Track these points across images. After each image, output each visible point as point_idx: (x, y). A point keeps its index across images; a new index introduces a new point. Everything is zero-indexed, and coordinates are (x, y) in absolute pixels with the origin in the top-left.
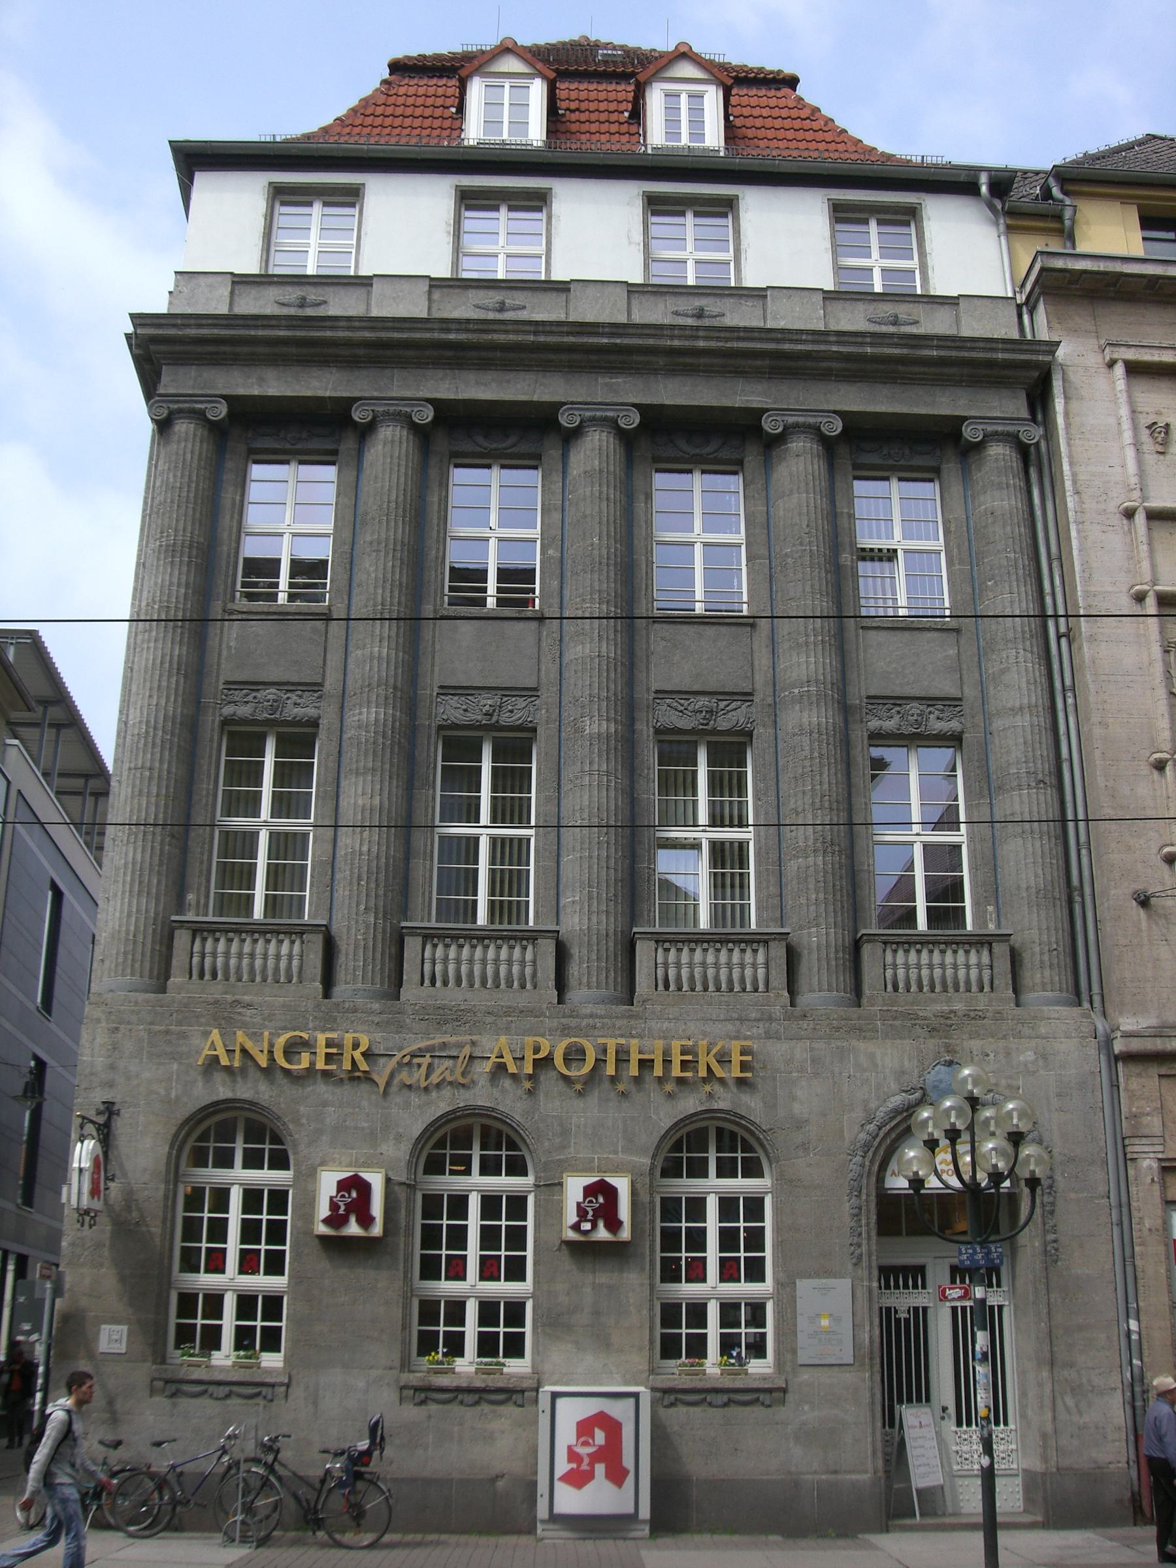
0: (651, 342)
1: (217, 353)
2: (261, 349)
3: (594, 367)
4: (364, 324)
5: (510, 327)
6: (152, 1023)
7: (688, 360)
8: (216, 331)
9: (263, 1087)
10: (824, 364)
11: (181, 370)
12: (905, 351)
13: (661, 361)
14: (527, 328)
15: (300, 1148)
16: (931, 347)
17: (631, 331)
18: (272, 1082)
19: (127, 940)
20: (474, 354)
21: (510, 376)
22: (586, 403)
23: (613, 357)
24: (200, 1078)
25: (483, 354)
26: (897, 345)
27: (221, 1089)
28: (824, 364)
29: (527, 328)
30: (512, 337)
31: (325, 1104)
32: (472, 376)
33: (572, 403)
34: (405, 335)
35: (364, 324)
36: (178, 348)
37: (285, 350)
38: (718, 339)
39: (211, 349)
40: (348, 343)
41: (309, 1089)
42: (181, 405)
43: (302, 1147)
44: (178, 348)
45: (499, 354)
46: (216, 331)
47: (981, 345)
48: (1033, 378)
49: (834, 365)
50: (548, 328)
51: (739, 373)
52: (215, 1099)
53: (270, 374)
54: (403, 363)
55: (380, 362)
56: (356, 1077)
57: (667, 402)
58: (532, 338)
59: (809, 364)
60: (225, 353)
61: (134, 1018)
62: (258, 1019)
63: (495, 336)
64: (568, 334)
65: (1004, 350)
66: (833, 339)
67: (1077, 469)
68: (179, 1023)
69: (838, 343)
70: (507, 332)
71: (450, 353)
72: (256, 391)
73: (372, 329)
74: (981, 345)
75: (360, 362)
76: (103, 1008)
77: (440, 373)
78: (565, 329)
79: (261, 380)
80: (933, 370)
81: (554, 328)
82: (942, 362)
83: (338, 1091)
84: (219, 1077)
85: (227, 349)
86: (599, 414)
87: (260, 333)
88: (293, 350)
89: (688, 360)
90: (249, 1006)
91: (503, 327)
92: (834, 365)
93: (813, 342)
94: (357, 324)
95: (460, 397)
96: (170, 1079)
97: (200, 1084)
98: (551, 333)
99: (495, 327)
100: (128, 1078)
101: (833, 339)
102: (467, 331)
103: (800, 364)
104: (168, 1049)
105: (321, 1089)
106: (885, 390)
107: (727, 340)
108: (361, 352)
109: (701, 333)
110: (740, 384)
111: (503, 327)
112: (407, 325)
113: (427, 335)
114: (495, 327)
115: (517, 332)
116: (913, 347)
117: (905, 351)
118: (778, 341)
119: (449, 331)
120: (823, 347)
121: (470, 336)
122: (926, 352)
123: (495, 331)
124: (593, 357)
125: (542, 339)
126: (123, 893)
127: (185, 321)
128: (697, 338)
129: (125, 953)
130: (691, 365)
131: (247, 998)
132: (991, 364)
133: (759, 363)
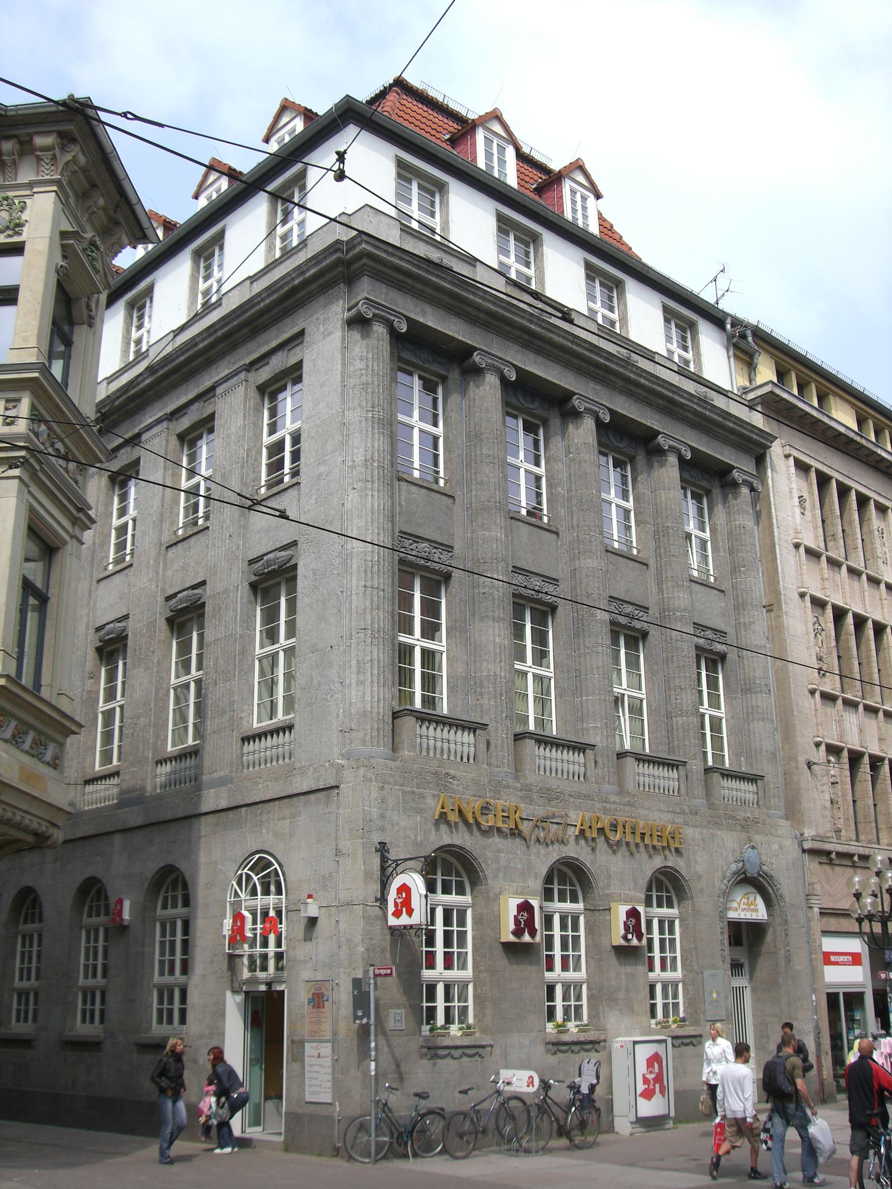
0: (621, 370)
1: (403, 282)
2: (429, 290)
3: (589, 374)
4: (491, 299)
5: (561, 333)
6: (402, 785)
7: (633, 388)
8: (409, 267)
9: (467, 836)
10: (686, 414)
11: (378, 285)
12: (721, 419)
13: (620, 383)
14: (570, 337)
15: (493, 881)
16: (730, 421)
17: (615, 360)
18: (471, 833)
19: (379, 719)
20: (538, 342)
21: (550, 363)
22: (596, 402)
23: (600, 372)
24: (433, 828)
25: (543, 345)
26: (719, 415)
27: (445, 837)
28: (686, 414)
29: (570, 337)
30: (560, 340)
31: (499, 851)
32: (532, 356)
33: (580, 395)
34: (510, 316)
35: (491, 299)
36: (381, 268)
37: (441, 296)
38: (650, 381)
39: (401, 277)
40: (478, 308)
41: (491, 840)
42: (383, 313)
43: (489, 881)
44: (381, 268)
45: (549, 348)
46: (409, 267)
47: (749, 427)
48: (756, 449)
49: (690, 416)
50: (579, 342)
51: (649, 404)
52: (442, 844)
53: (429, 309)
54: (499, 333)
55: (487, 326)
56: (515, 833)
57: (619, 411)
58: (570, 344)
59: (680, 411)
60: (407, 284)
61: (392, 780)
62: (460, 788)
63: (553, 336)
64: (587, 349)
65: (757, 434)
66: (696, 401)
67: (778, 514)
68: (418, 787)
69: (697, 404)
70: (559, 335)
71: (526, 337)
72: (421, 320)
73: (494, 304)
74: (749, 427)
75: (477, 322)
76: (372, 770)
77: (516, 347)
78: (587, 346)
79: (424, 313)
80: (724, 433)
81: (582, 344)
82: (732, 431)
83: (505, 842)
84: (443, 828)
85: (409, 281)
86: (592, 407)
87: (434, 279)
88: (446, 299)
89: (633, 388)
90: (454, 778)
91: (558, 332)
92: (690, 416)
93: (687, 399)
94: (488, 297)
95: (527, 368)
96: (416, 827)
97: (433, 832)
98: (579, 345)
99: (555, 330)
100: (392, 825)
101: (696, 401)
102: (541, 326)
103: (677, 409)
104: (414, 805)
105: (496, 840)
106: (705, 438)
107: (654, 383)
108: (482, 316)
109: (644, 374)
110: (648, 412)
111: (558, 332)
112: (513, 310)
113: (521, 321)
114: (555, 330)
115: (564, 338)
116: (724, 418)
117: (721, 419)
118: (673, 392)
119: (531, 322)
120: (691, 404)
121: (538, 329)
122: (729, 424)
123: (554, 333)
124: (592, 369)
125: (575, 347)
126: (372, 682)
127: (394, 251)
128: (641, 376)
129: (378, 730)
130: (632, 391)
131: (452, 772)
132: (749, 439)
133: (661, 402)
